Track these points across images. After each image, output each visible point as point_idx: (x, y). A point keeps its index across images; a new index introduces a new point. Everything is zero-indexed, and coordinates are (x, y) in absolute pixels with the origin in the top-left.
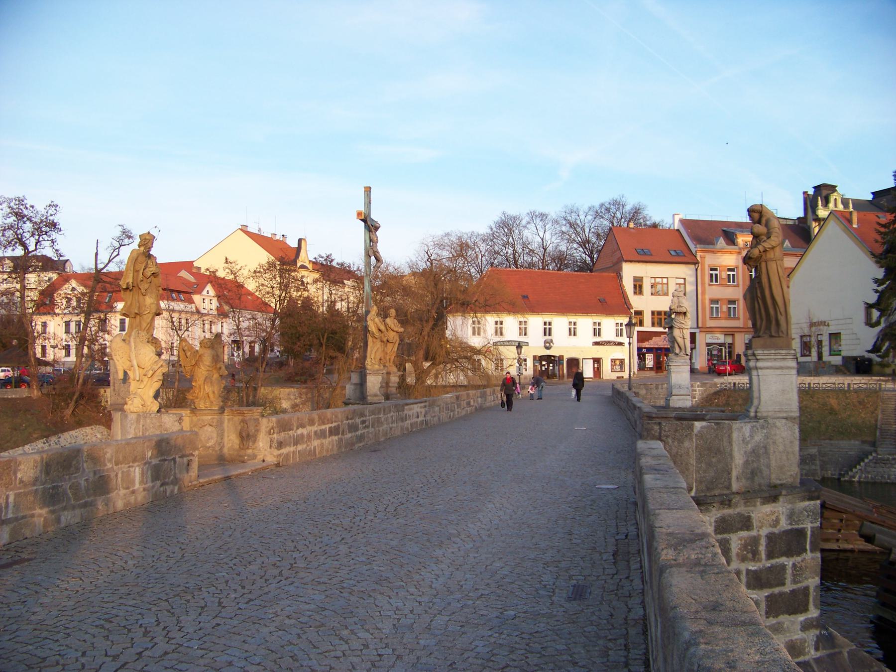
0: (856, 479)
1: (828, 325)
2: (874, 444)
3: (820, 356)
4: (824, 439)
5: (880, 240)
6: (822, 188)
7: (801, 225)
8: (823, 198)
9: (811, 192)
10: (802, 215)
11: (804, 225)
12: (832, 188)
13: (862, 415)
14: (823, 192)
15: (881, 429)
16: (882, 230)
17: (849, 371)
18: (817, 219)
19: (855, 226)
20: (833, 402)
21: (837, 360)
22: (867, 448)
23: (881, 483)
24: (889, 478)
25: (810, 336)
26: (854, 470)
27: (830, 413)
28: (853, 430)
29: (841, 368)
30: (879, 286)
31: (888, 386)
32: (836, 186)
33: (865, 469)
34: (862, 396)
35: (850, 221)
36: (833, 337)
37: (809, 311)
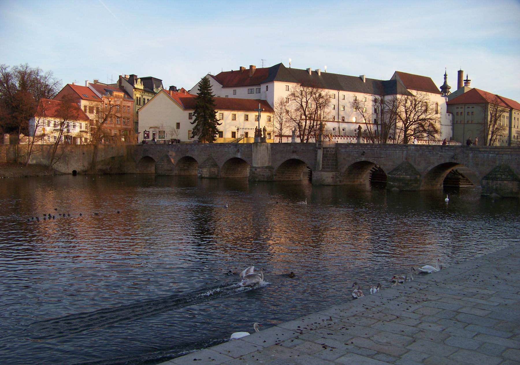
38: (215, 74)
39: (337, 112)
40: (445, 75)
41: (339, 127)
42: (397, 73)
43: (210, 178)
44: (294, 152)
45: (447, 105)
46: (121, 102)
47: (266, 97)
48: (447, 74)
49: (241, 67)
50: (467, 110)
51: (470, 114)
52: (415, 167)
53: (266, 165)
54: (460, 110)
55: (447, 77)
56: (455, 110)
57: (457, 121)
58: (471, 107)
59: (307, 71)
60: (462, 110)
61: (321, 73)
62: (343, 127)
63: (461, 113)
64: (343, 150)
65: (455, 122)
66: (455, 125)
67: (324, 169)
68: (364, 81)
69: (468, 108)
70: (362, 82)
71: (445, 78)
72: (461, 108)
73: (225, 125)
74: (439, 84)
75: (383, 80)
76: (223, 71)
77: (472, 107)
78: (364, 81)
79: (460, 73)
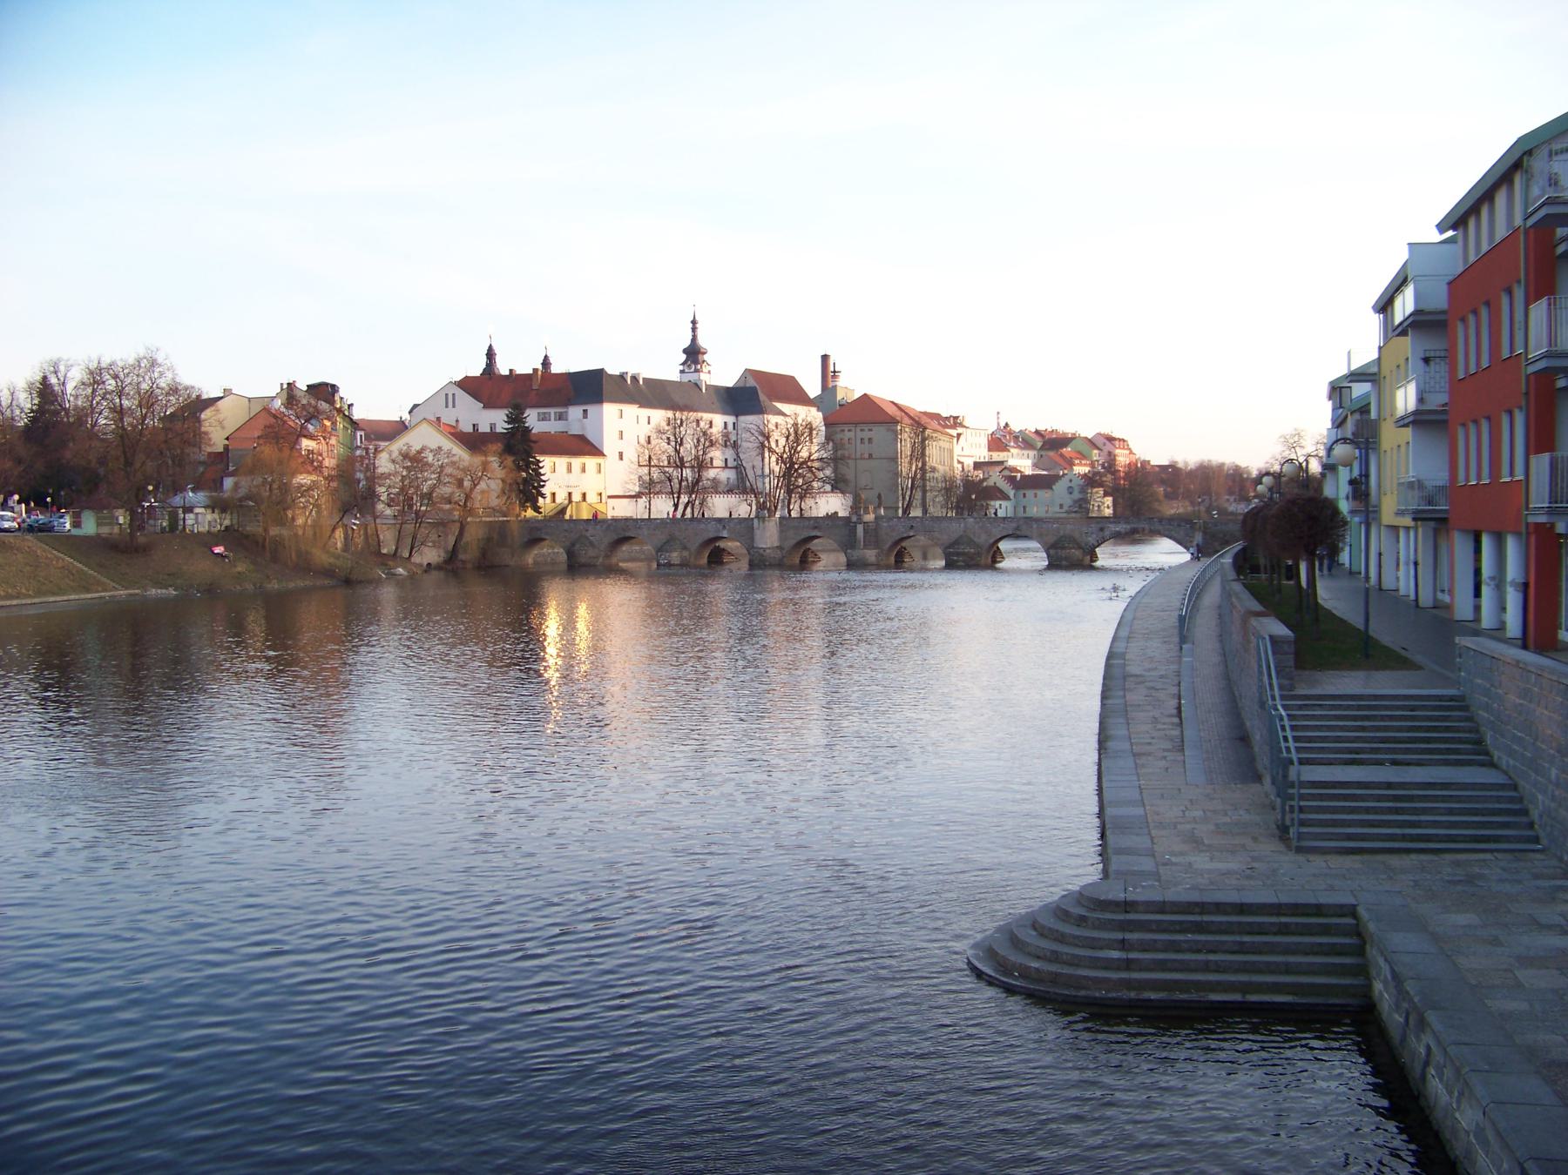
40: (694, 322)
43: (681, 565)
44: (816, 528)
47: (583, 428)
48: (697, 318)
49: (511, 371)
50: (860, 435)
51: (866, 441)
52: (976, 540)
53: (776, 544)
55: (698, 325)
58: (866, 429)
60: (851, 434)
61: (644, 379)
64: (885, 524)
67: (866, 546)
69: (862, 430)
71: (694, 329)
72: (849, 431)
74: (813, 388)
76: (469, 375)
77: (870, 430)
79: (825, 358)
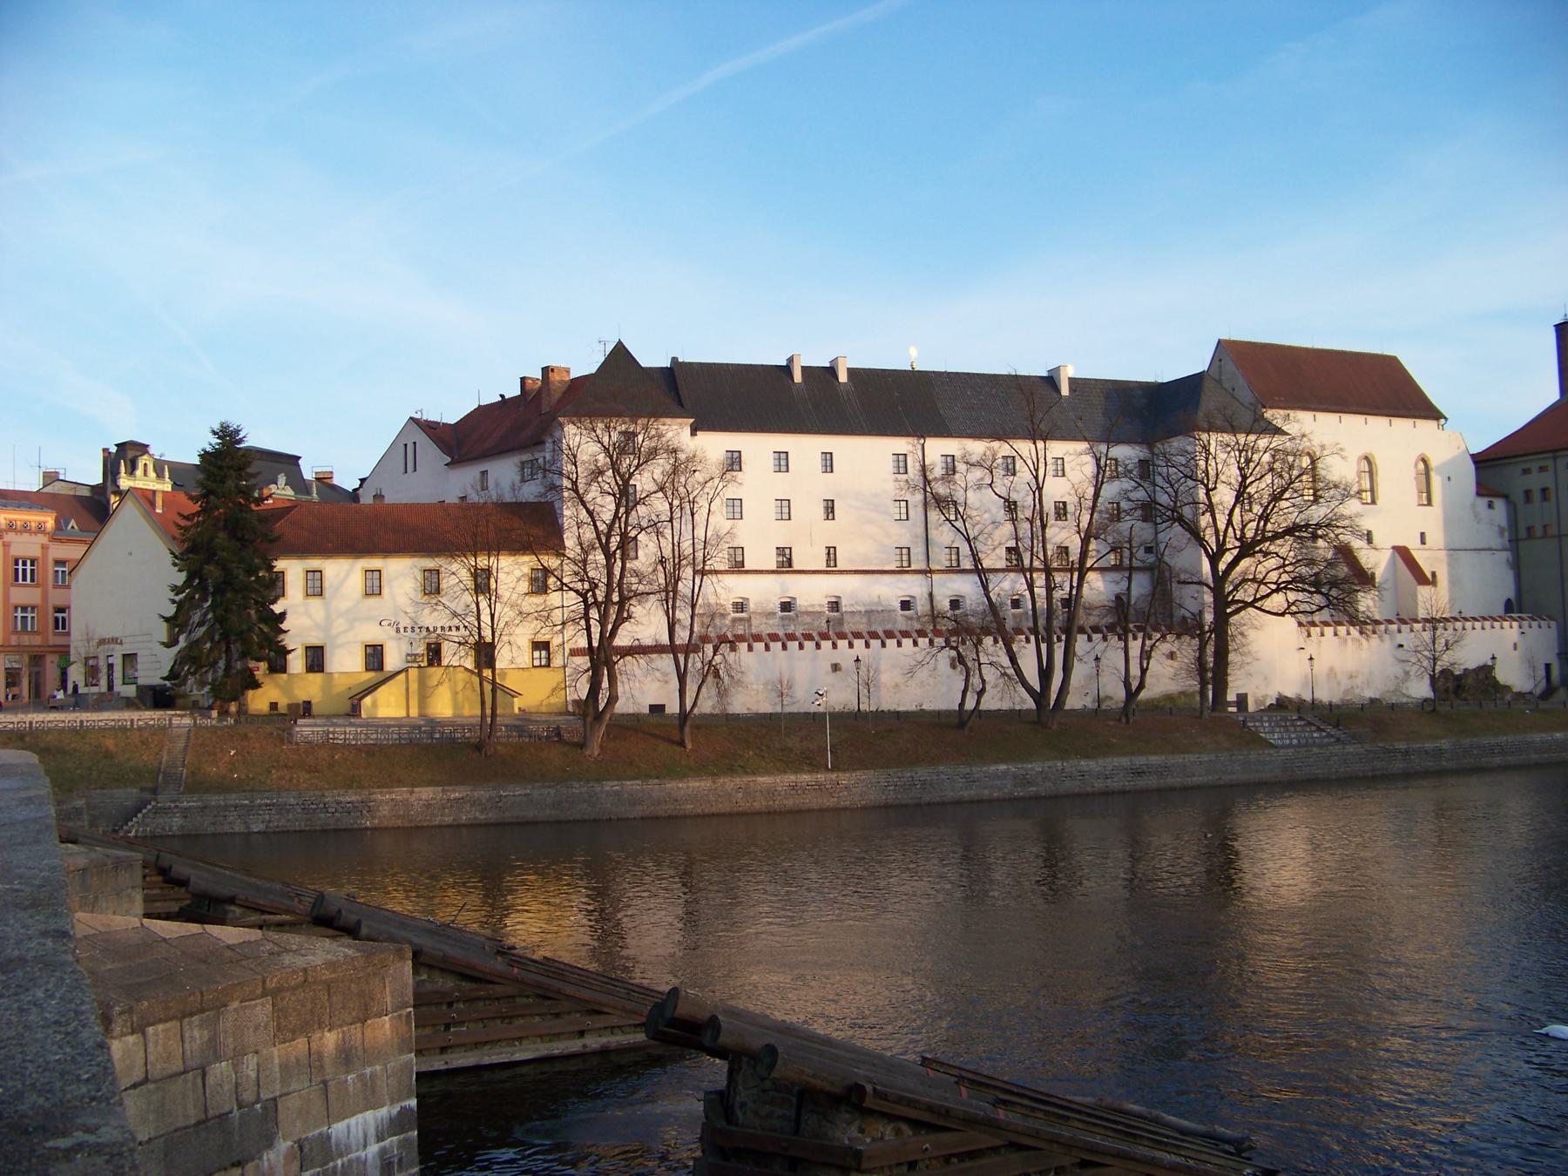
0: (132, 834)
1: (121, 643)
2: (154, 791)
3: (111, 687)
4: (95, 789)
5: (178, 536)
6: (127, 447)
7: (96, 497)
8: (129, 463)
9: (114, 449)
10: (99, 480)
11: (102, 498)
12: (143, 449)
13: (145, 758)
14: (126, 455)
15: (164, 773)
16: (183, 523)
17: (145, 705)
18: (118, 492)
19: (159, 511)
20: (109, 743)
21: (130, 691)
22: (147, 796)
23: (161, 836)
24: (170, 830)
25: (96, 657)
26: (130, 824)
27: (105, 757)
28: (132, 776)
29: (136, 701)
30: (177, 594)
31: (183, 722)
32: (148, 446)
33: (143, 820)
34: (146, 735)
35: (153, 504)
36: (126, 658)
37: (87, 627)
38: (451, 412)
39: (920, 530)
41: (931, 595)
42: (1225, 349)
45: (1475, 463)
46: (44, 548)
49: (523, 380)
54: (1536, 481)
56: (1517, 481)
57: (1529, 529)
59: (786, 370)
62: (950, 593)
63: (1544, 490)
65: (1523, 534)
66: (1522, 545)
68: (1065, 391)
70: (1055, 395)
72: (1542, 469)
73: (329, 621)
75: (1160, 380)
78: (1065, 391)
